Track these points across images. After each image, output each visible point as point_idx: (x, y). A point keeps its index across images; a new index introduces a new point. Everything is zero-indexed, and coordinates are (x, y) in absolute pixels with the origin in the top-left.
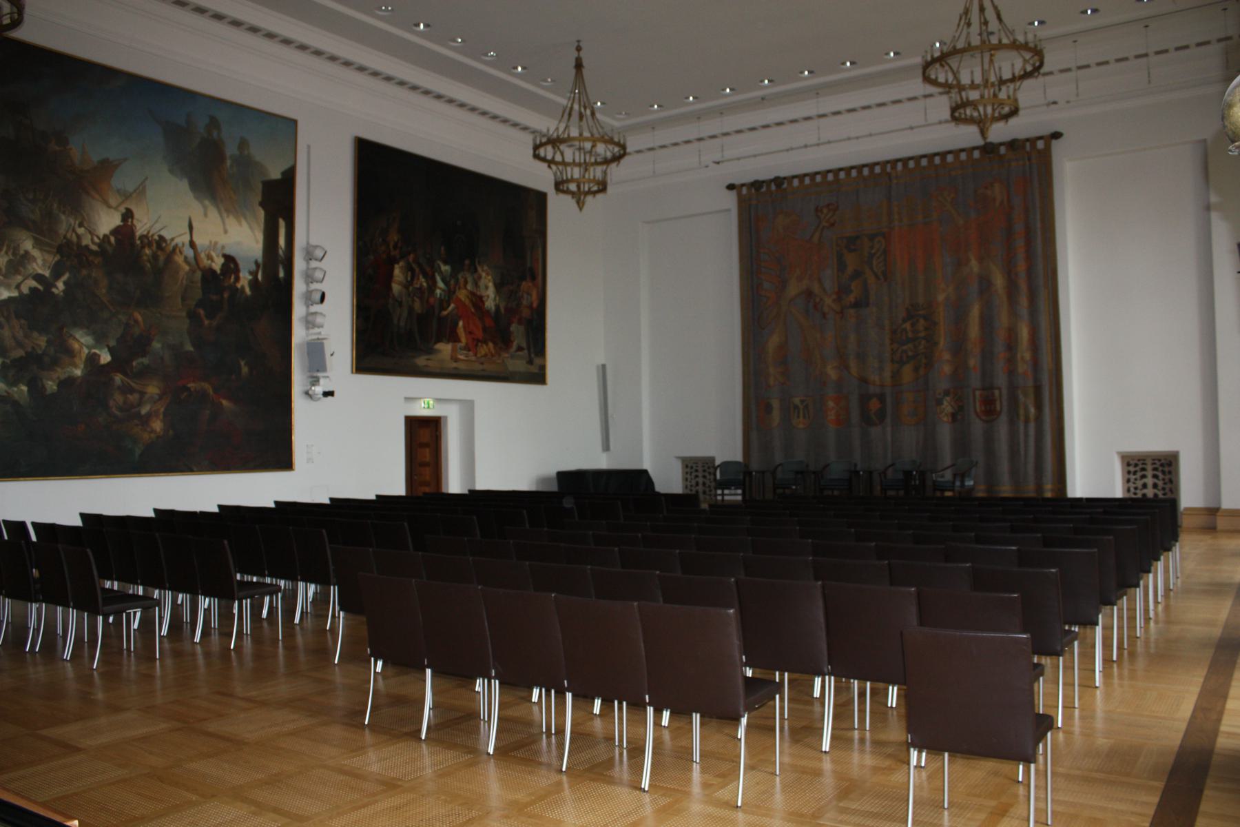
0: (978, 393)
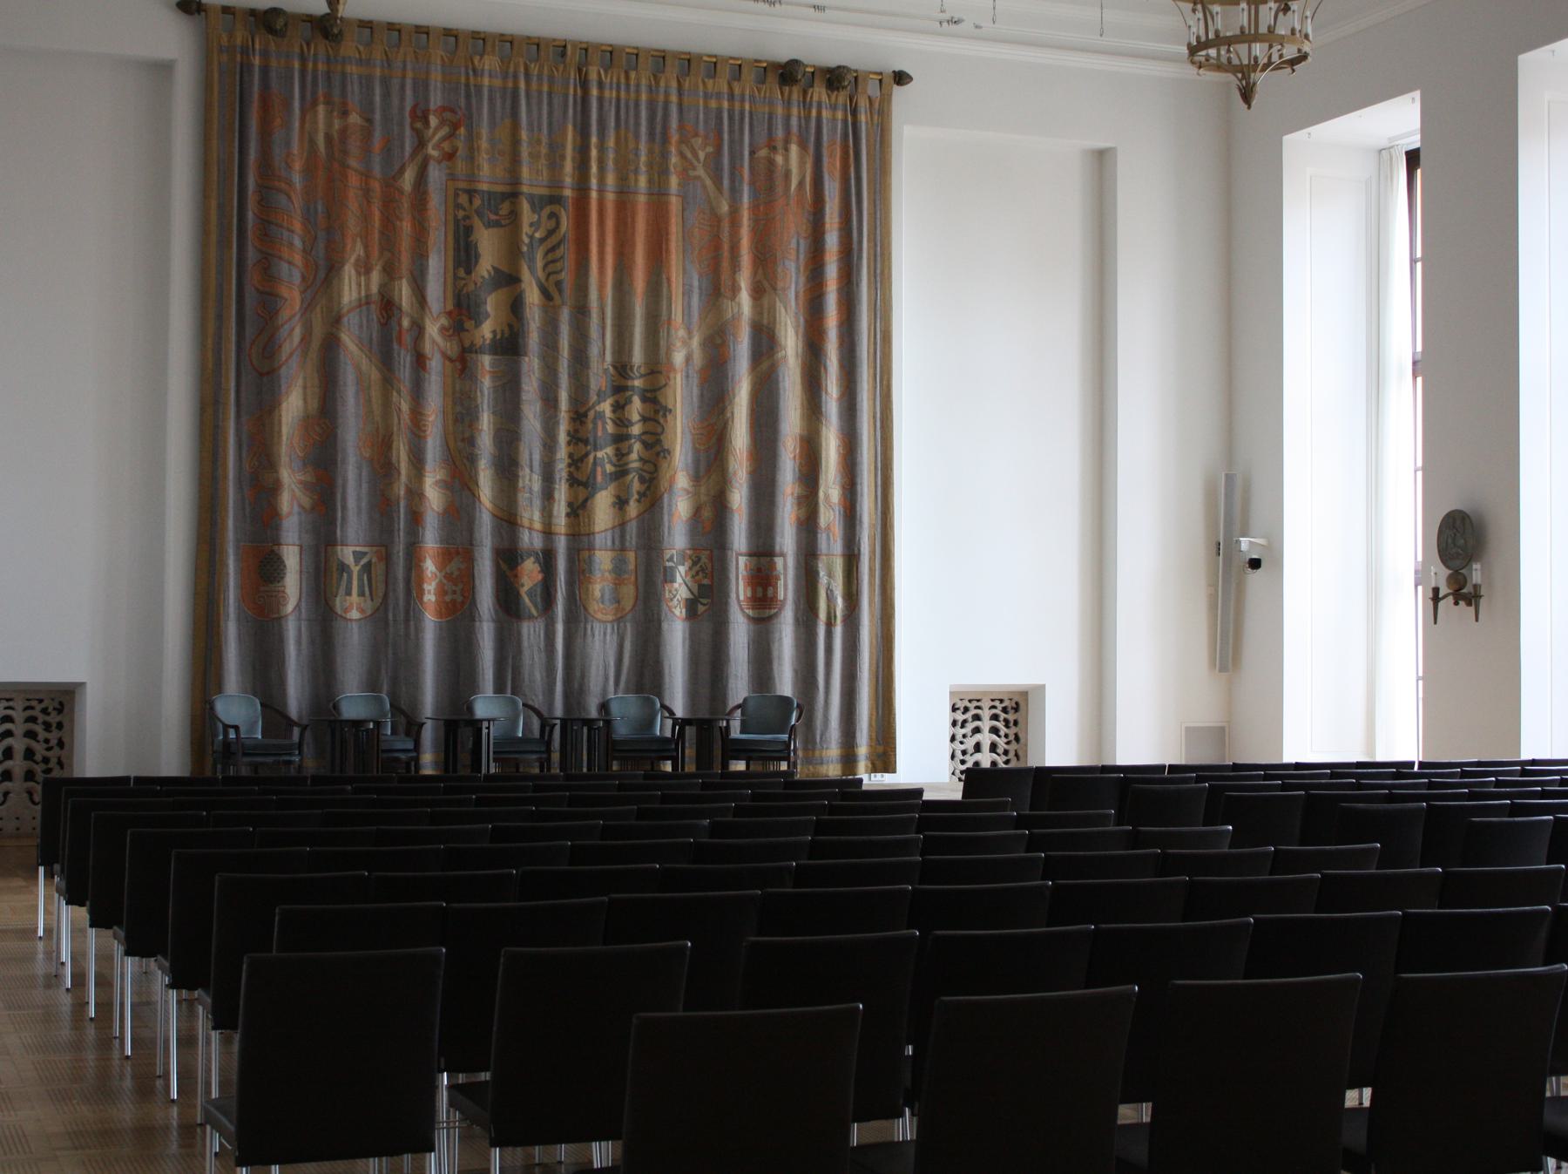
0: (742, 560)
